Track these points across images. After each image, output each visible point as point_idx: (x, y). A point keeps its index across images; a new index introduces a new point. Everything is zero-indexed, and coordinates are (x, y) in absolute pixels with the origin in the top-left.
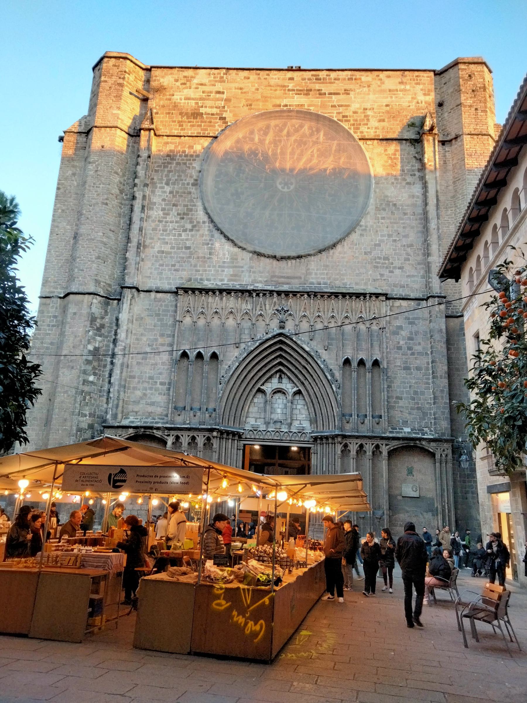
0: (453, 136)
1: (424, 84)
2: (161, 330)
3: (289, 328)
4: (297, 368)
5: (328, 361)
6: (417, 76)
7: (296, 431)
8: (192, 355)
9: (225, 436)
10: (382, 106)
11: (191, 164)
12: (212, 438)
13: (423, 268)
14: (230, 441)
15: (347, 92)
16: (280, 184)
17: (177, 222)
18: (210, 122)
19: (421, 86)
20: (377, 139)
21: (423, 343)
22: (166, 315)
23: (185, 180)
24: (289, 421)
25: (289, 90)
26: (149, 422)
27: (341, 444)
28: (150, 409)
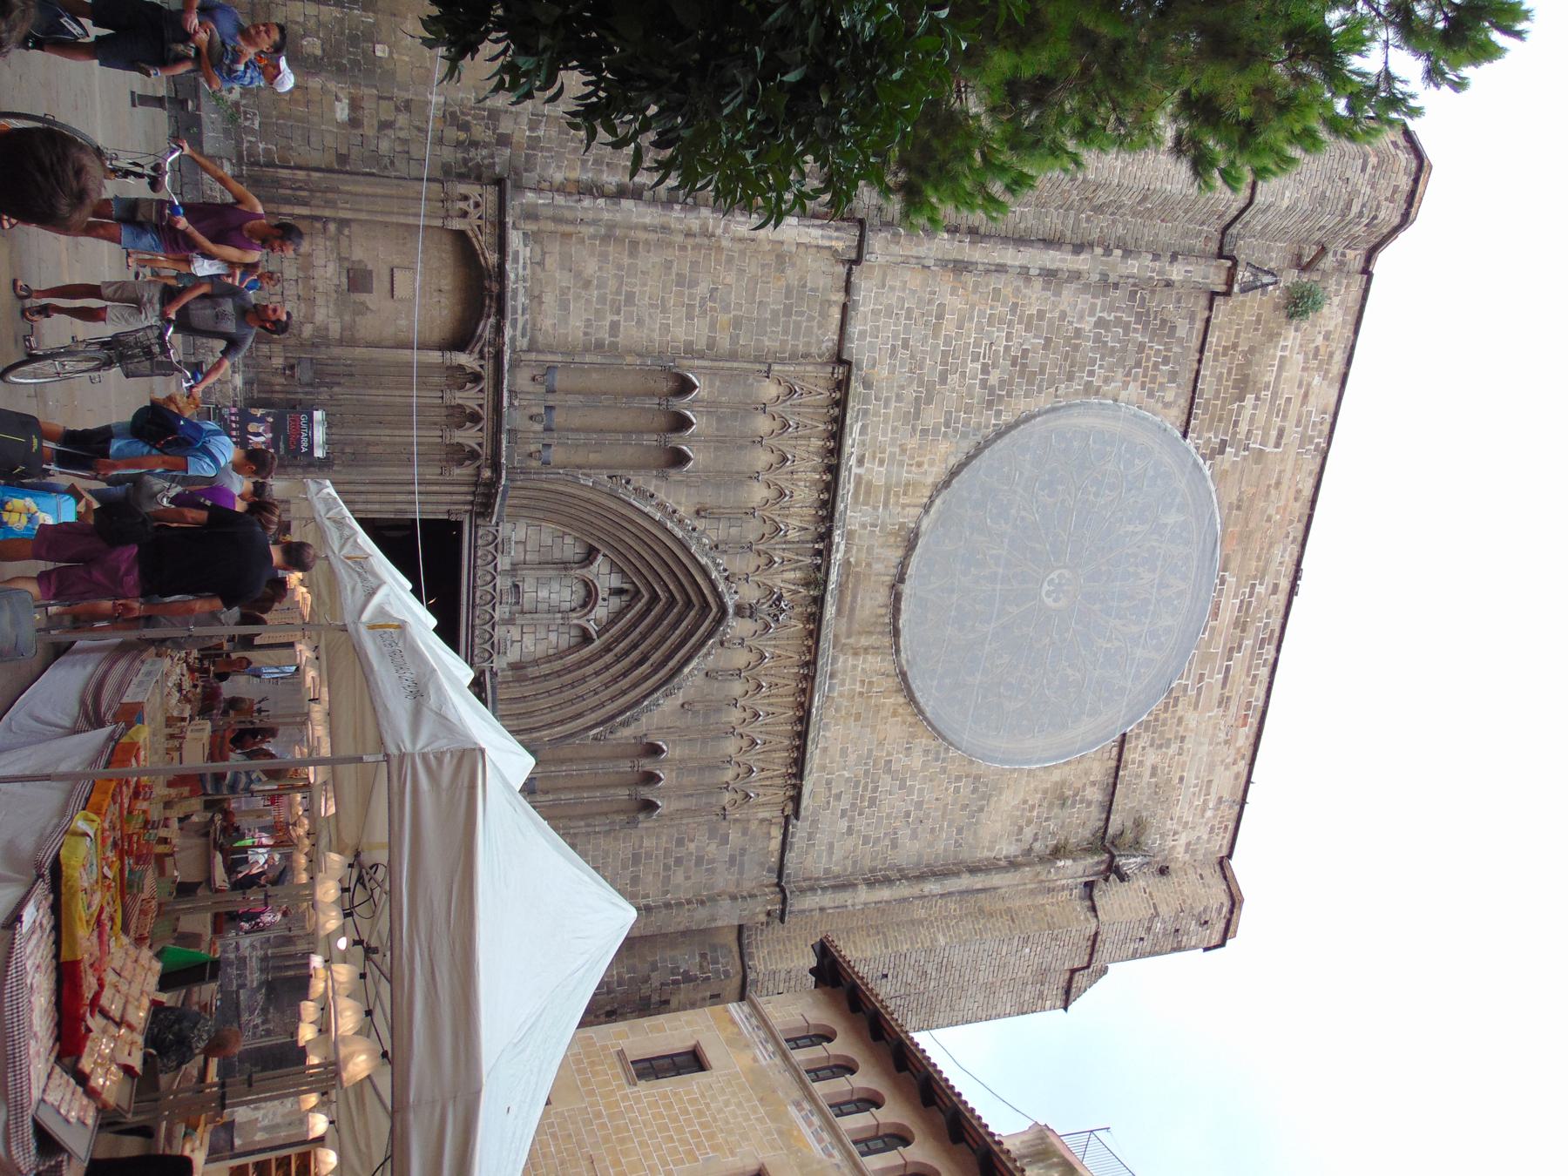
0: (1098, 904)
1: (1209, 841)
2: (749, 319)
3: (737, 627)
4: (644, 637)
5: (656, 712)
6: (1226, 827)
7: (496, 639)
8: (683, 405)
9: (480, 490)
10: (1183, 771)
11: (1135, 380)
12: (478, 463)
13: (845, 870)
15: (1224, 702)
16: (1060, 576)
17: (1007, 348)
18: (1220, 420)
19: (1205, 837)
20: (1118, 768)
21: (689, 883)
22: (786, 332)
23: (1101, 367)
25: (1253, 586)
26: (518, 299)
28: (549, 299)
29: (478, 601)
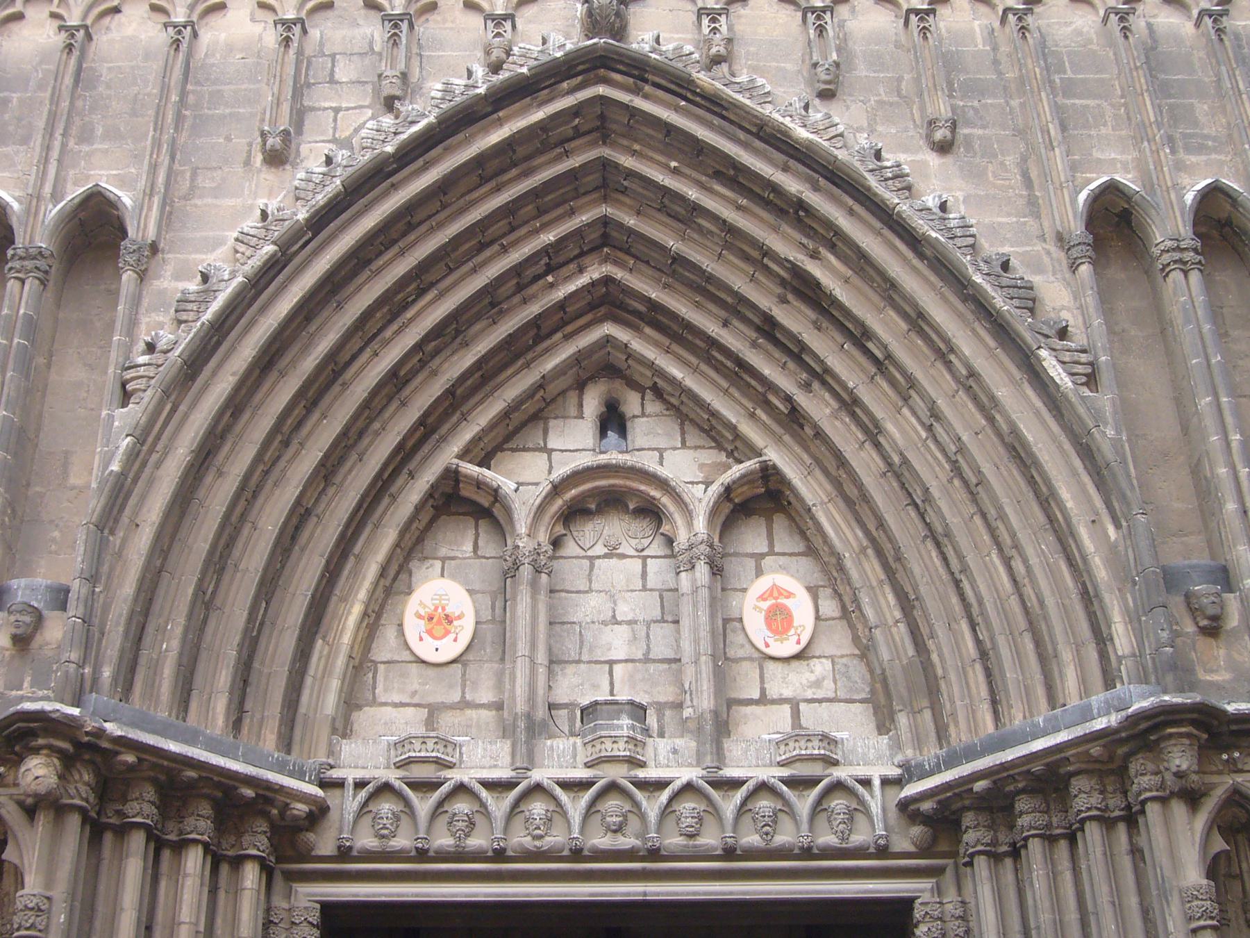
7: (771, 774)
14: (194, 860)
24: (705, 701)
27: (1193, 798)
29: (626, 841)
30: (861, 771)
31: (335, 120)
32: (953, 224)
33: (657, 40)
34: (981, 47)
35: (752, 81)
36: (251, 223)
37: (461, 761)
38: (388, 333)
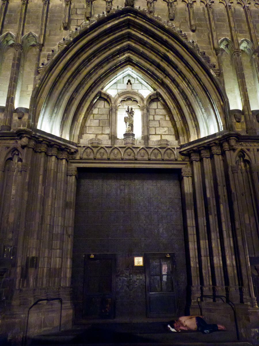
9: (43, 148)
12: (20, 149)
29: (131, 157)
30: (173, 147)
31: (77, 22)
32: (195, 45)
33: (140, 8)
34: (202, 11)
35: (158, 16)
36: (62, 41)
37: (102, 143)
38: (88, 64)
